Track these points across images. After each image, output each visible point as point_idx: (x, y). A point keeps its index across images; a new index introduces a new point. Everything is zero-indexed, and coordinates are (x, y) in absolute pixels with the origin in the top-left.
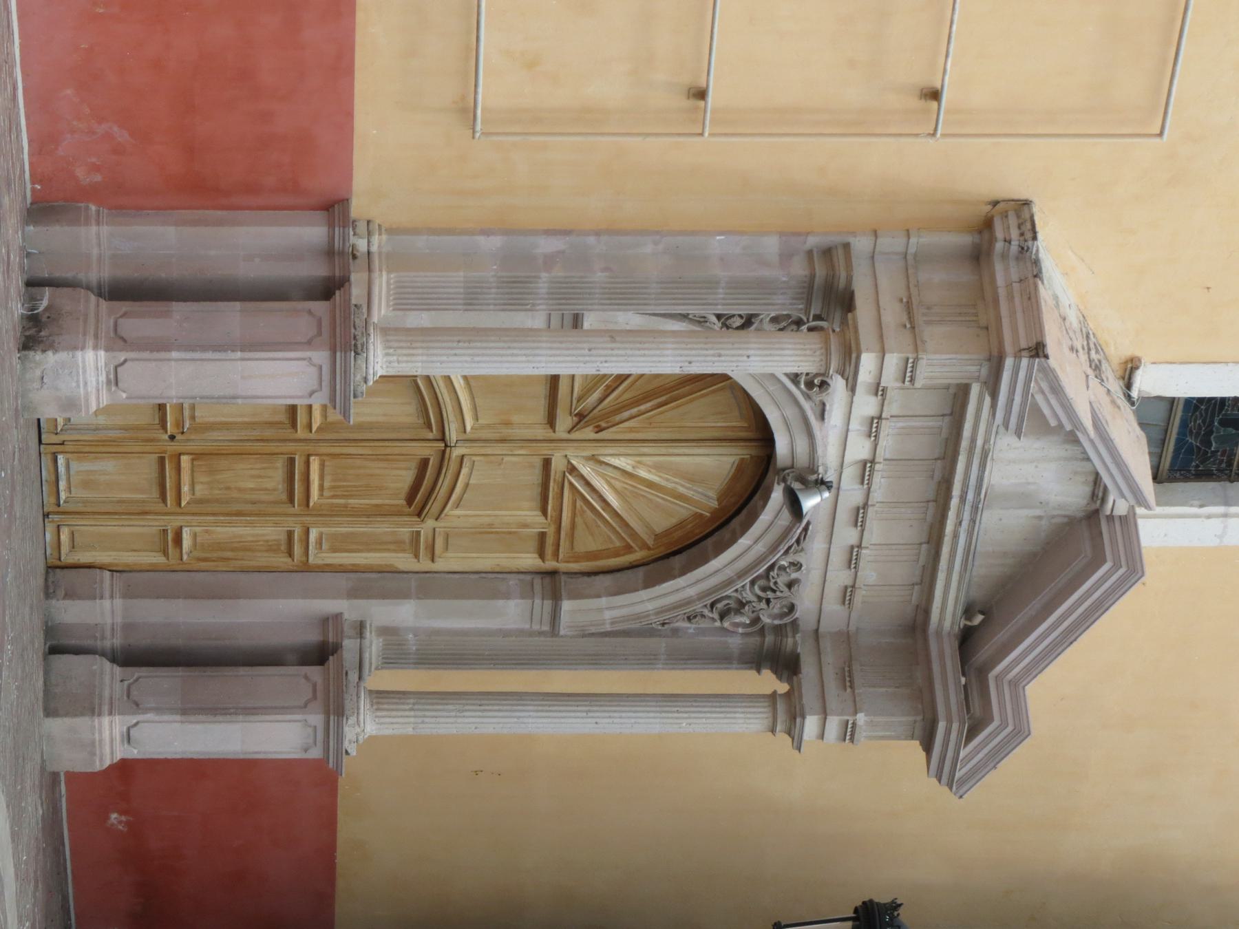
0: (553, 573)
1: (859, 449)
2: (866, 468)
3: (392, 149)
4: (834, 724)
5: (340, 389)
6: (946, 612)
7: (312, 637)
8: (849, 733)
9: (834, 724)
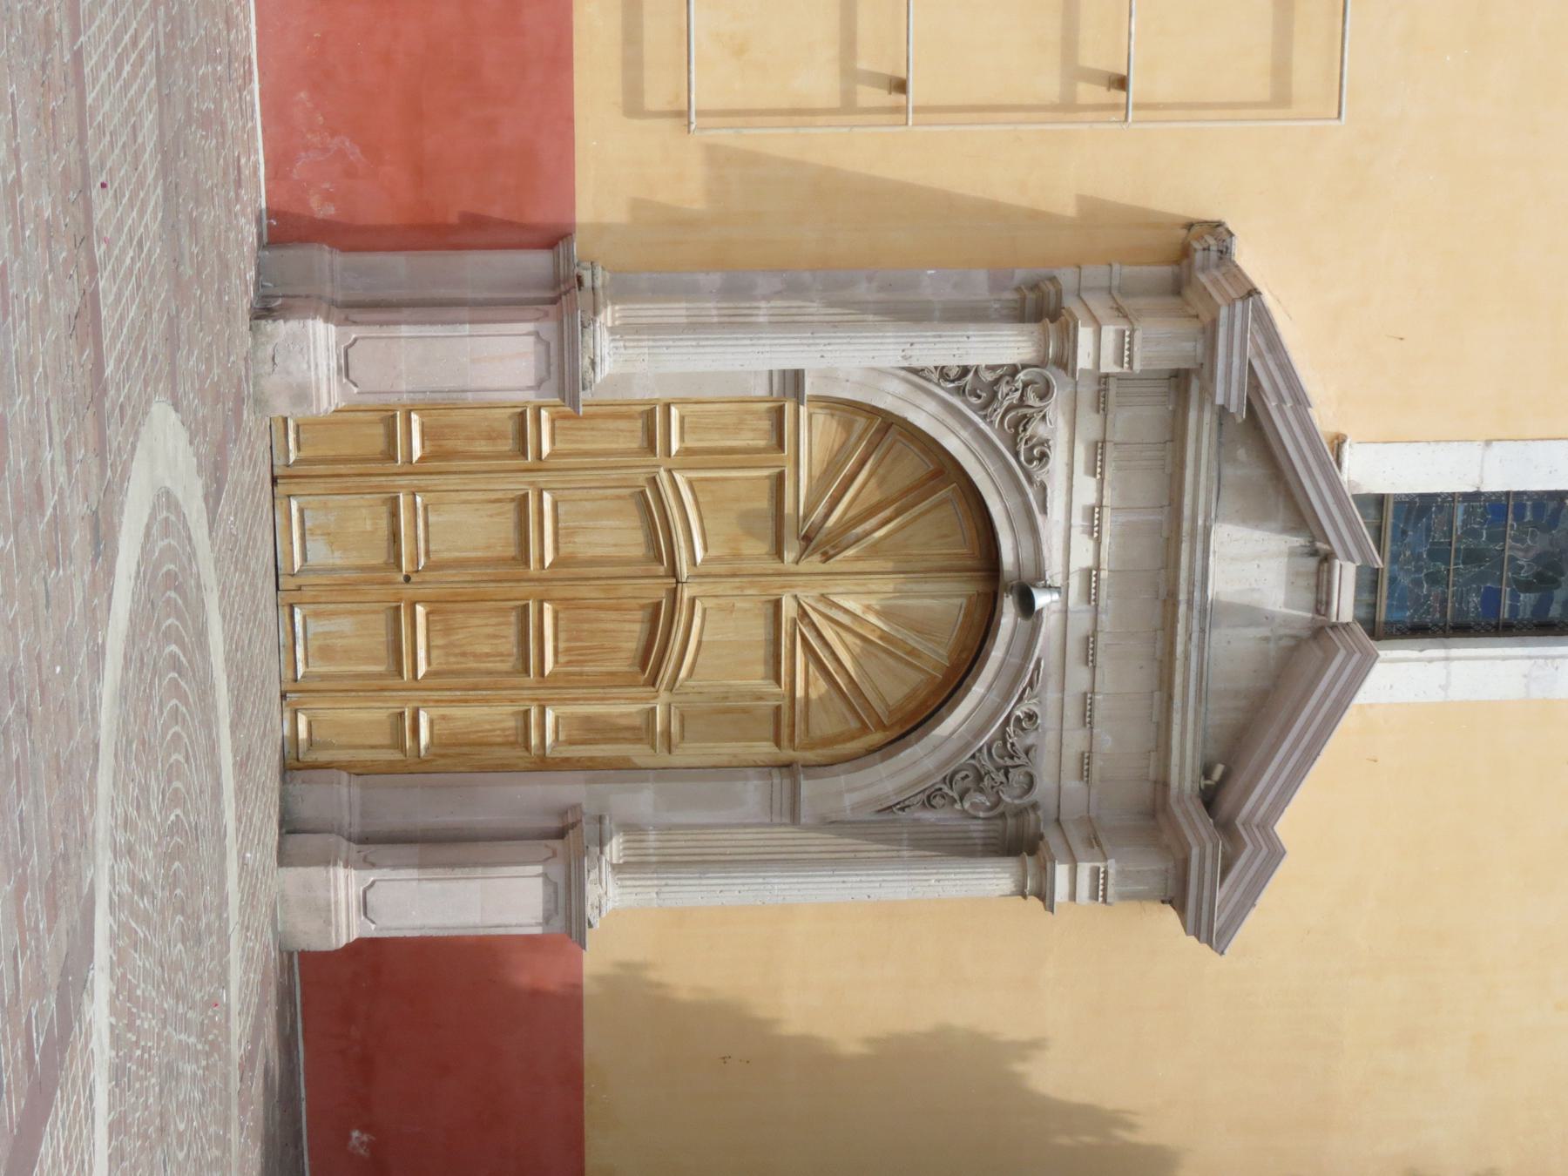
0: (788, 766)
1: (1083, 555)
2: (1090, 576)
3: (615, 169)
4: (1084, 870)
5: (564, 372)
6: (1184, 776)
7: (554, 824)
8: (1098, 892)
9: (1084, 870)
